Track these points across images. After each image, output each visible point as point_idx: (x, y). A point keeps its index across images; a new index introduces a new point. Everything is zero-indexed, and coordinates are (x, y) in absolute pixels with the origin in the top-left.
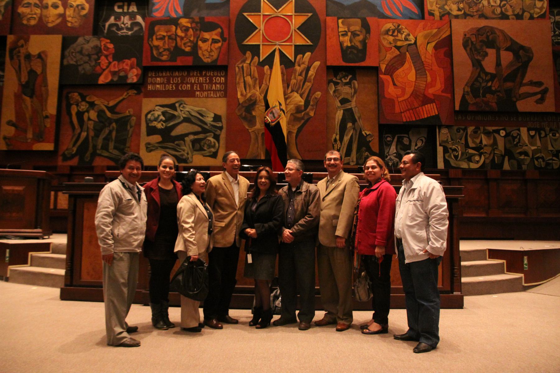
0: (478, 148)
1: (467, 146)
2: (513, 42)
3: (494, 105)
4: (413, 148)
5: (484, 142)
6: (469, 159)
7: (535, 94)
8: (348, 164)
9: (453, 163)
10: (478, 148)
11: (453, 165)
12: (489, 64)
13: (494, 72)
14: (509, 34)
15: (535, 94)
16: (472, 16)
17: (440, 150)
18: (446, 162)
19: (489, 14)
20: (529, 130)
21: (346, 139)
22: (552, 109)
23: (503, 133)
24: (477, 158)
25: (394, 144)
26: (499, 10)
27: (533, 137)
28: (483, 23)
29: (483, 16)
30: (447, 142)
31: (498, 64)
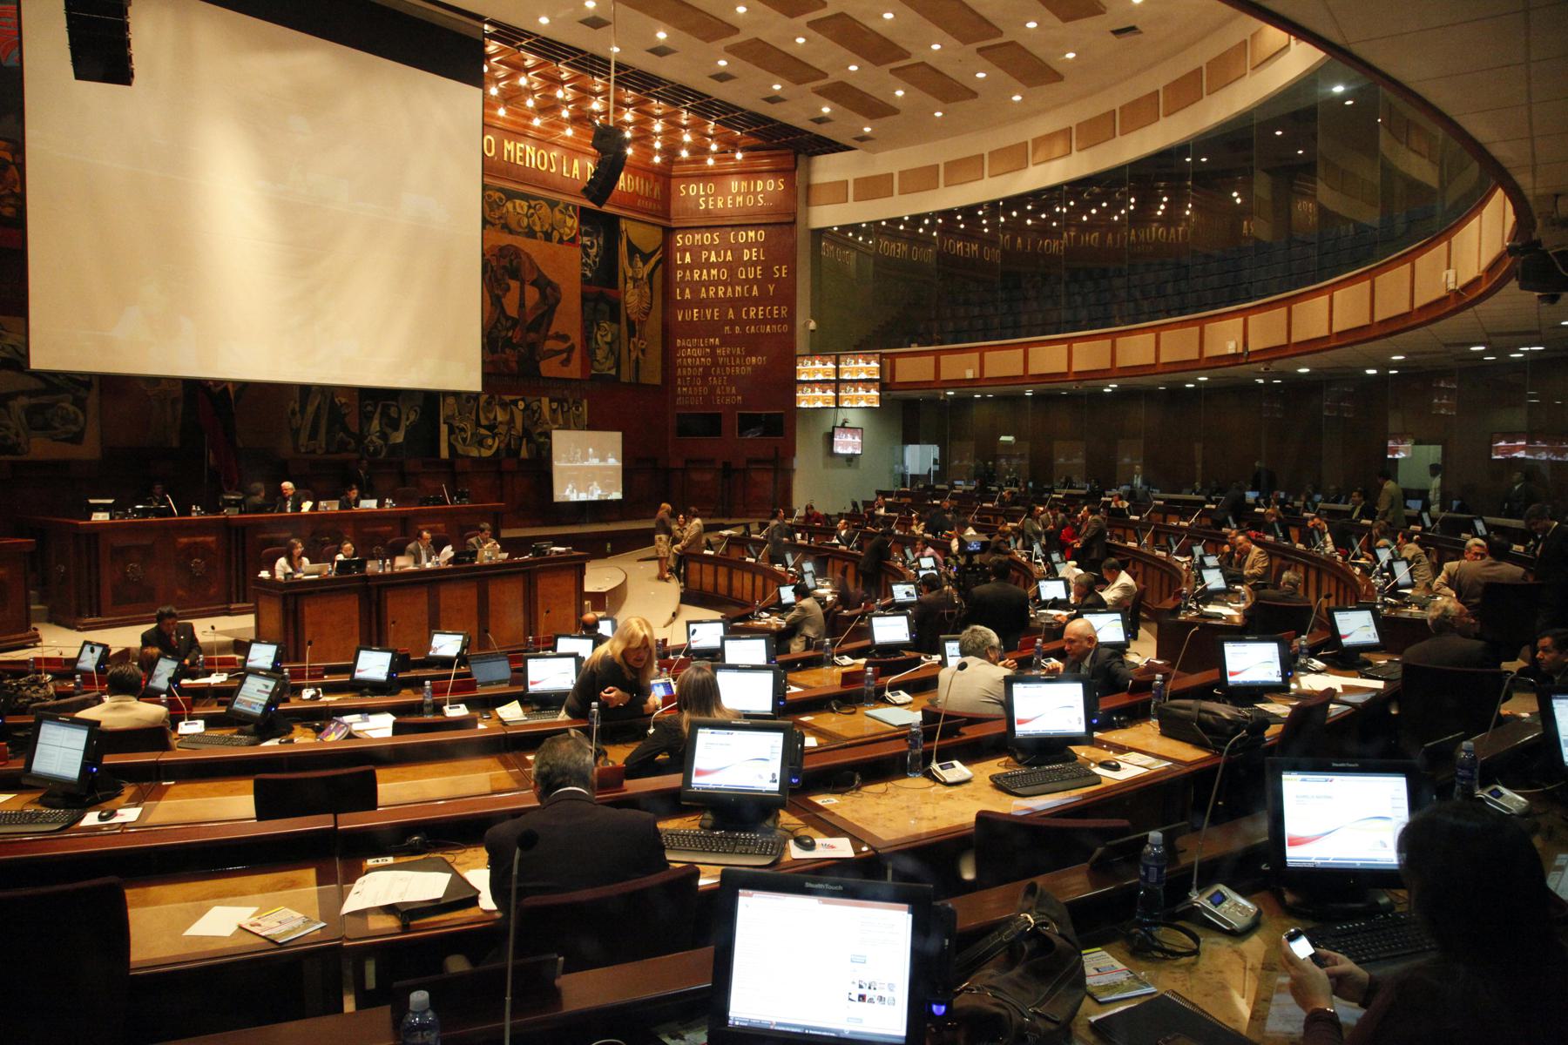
0: (492, 428)
1: (478, 424)
2: (541, 275)
3: (513, 365)
4: (404, 424)
5: (500, 418)
6: (481, 443)
7: (561, 352)
8: (314, 452)
9: (460, 449)
10: (492, 428)
11: (460, 451)
12: (511, 305)
13: (515, 315)
14: (538, 262)
15: (561, 352)
16: (493, 225)
17: (444, 429)
18: (451, 447)
19: (514, 225)
20: (551, 401)
21: (310, 409)
22: (578, 375)
23: (521, 405)
24: (490, 442)
25: (377, 416)
26: (525, 222)
27: (554, 411)
28: (506, 239)
29: (506, 227)
30: (453, 417)
31: (522, 305)
